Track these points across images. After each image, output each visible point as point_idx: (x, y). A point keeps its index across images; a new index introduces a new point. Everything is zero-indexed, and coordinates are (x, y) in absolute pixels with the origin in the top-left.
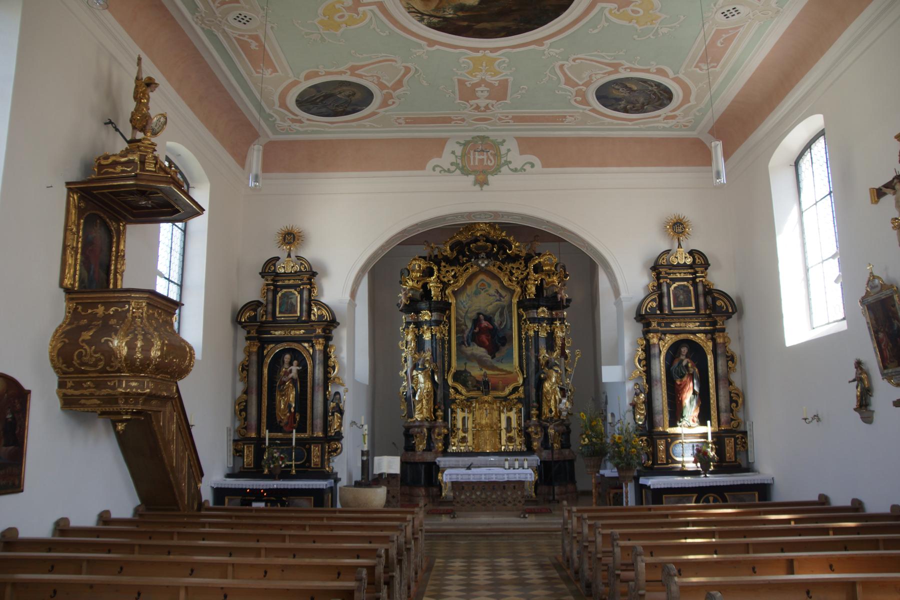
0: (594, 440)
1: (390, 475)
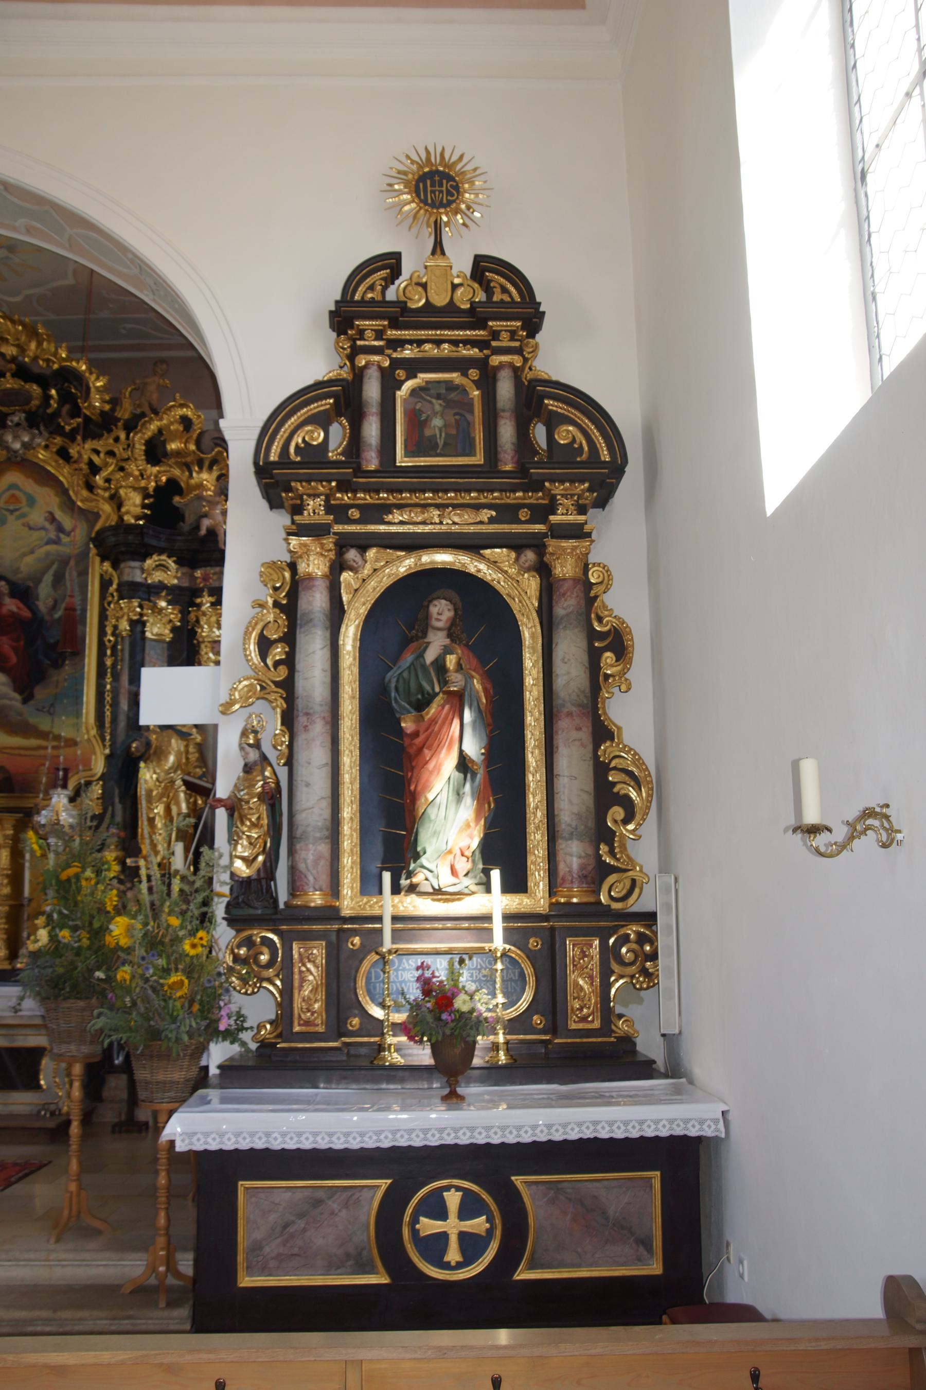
0: (65, 935)
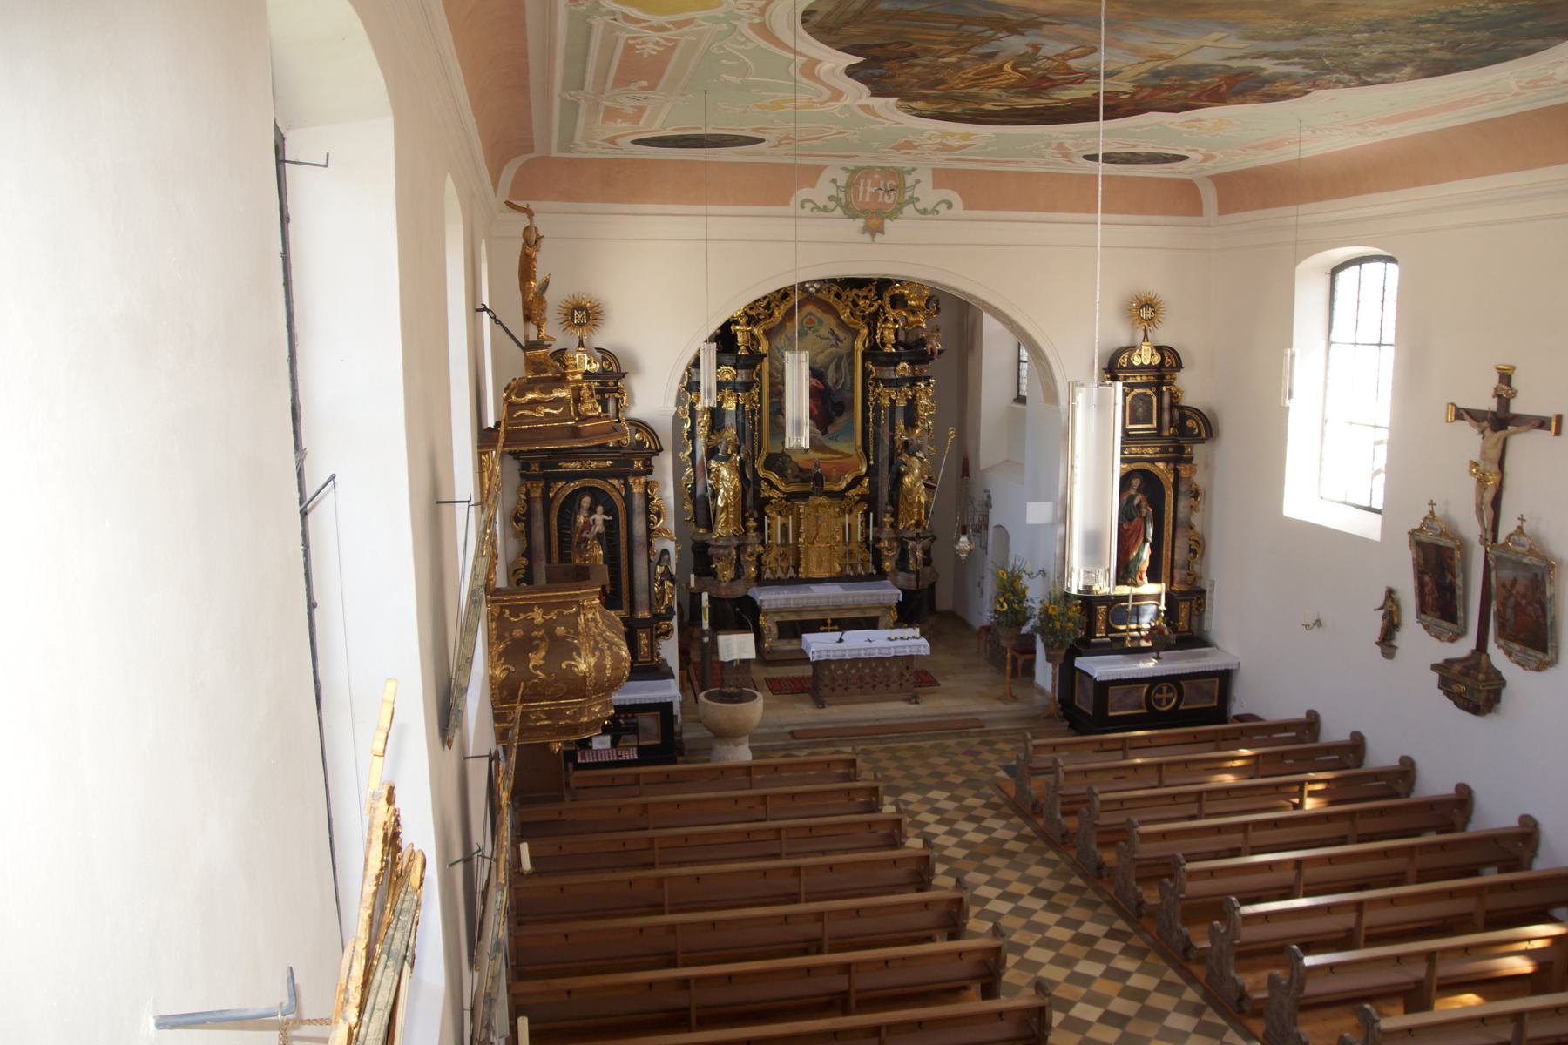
1: (743, 661)
